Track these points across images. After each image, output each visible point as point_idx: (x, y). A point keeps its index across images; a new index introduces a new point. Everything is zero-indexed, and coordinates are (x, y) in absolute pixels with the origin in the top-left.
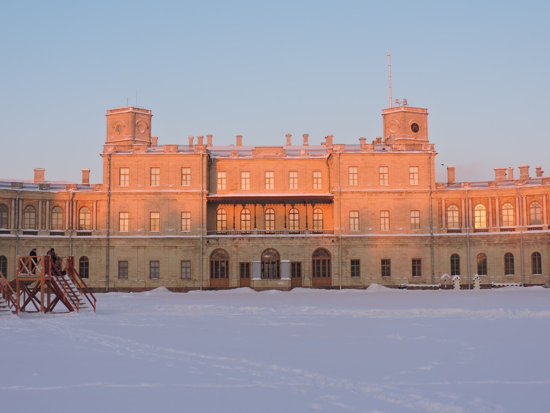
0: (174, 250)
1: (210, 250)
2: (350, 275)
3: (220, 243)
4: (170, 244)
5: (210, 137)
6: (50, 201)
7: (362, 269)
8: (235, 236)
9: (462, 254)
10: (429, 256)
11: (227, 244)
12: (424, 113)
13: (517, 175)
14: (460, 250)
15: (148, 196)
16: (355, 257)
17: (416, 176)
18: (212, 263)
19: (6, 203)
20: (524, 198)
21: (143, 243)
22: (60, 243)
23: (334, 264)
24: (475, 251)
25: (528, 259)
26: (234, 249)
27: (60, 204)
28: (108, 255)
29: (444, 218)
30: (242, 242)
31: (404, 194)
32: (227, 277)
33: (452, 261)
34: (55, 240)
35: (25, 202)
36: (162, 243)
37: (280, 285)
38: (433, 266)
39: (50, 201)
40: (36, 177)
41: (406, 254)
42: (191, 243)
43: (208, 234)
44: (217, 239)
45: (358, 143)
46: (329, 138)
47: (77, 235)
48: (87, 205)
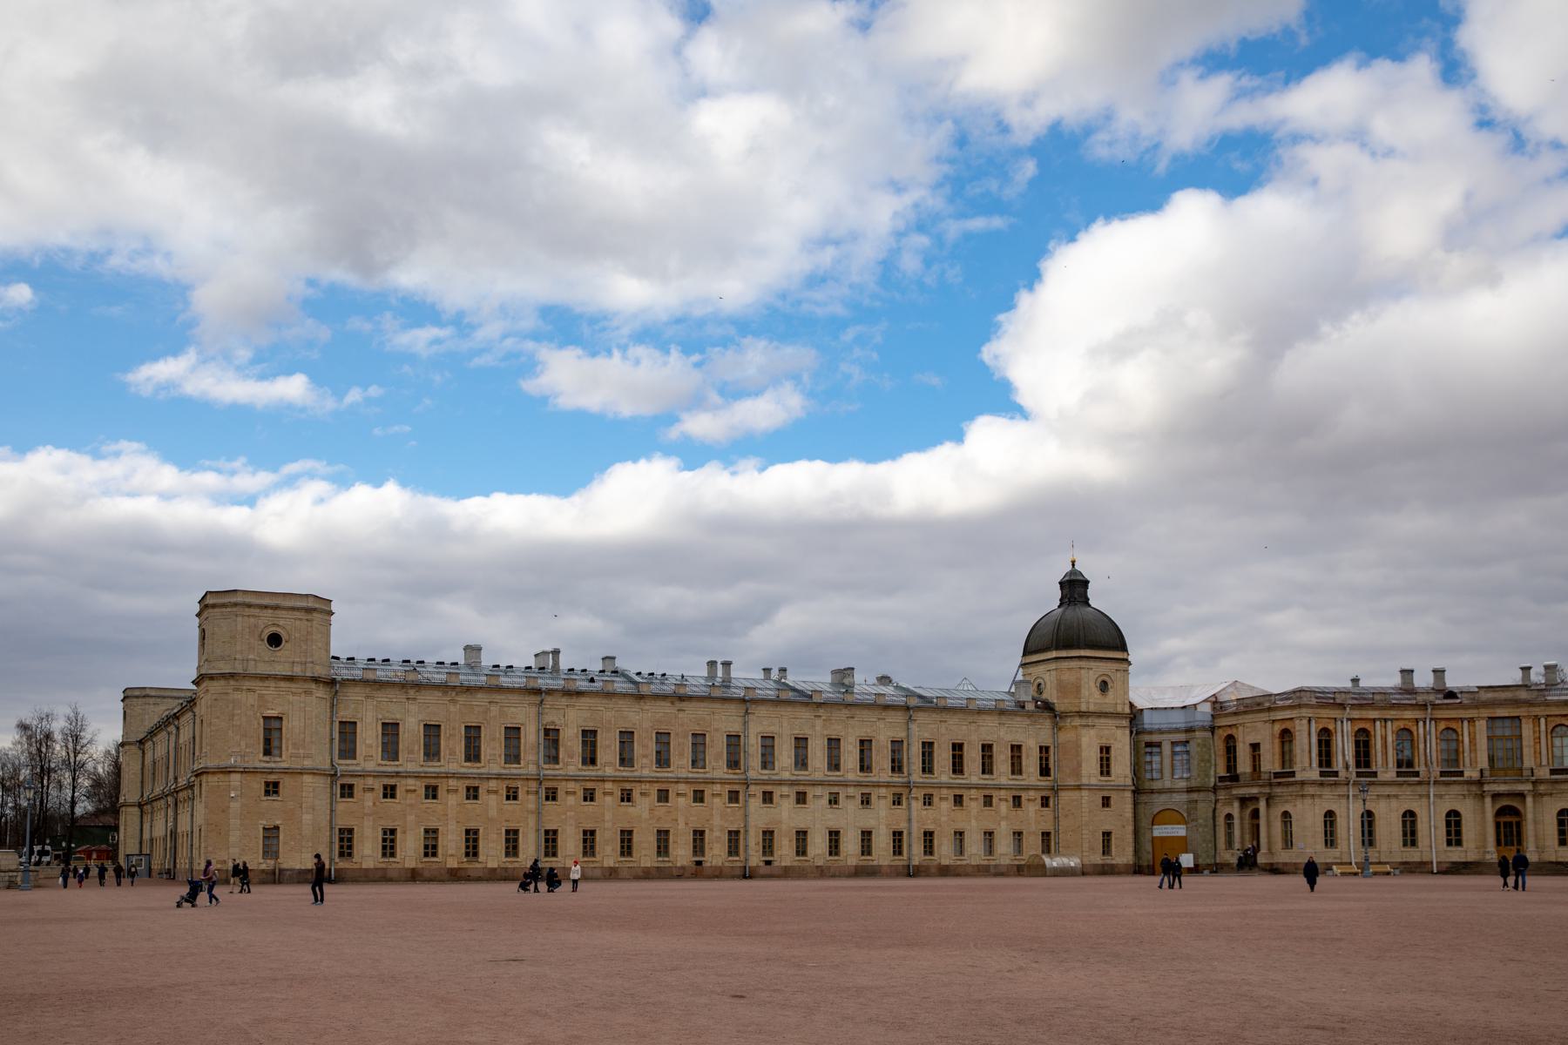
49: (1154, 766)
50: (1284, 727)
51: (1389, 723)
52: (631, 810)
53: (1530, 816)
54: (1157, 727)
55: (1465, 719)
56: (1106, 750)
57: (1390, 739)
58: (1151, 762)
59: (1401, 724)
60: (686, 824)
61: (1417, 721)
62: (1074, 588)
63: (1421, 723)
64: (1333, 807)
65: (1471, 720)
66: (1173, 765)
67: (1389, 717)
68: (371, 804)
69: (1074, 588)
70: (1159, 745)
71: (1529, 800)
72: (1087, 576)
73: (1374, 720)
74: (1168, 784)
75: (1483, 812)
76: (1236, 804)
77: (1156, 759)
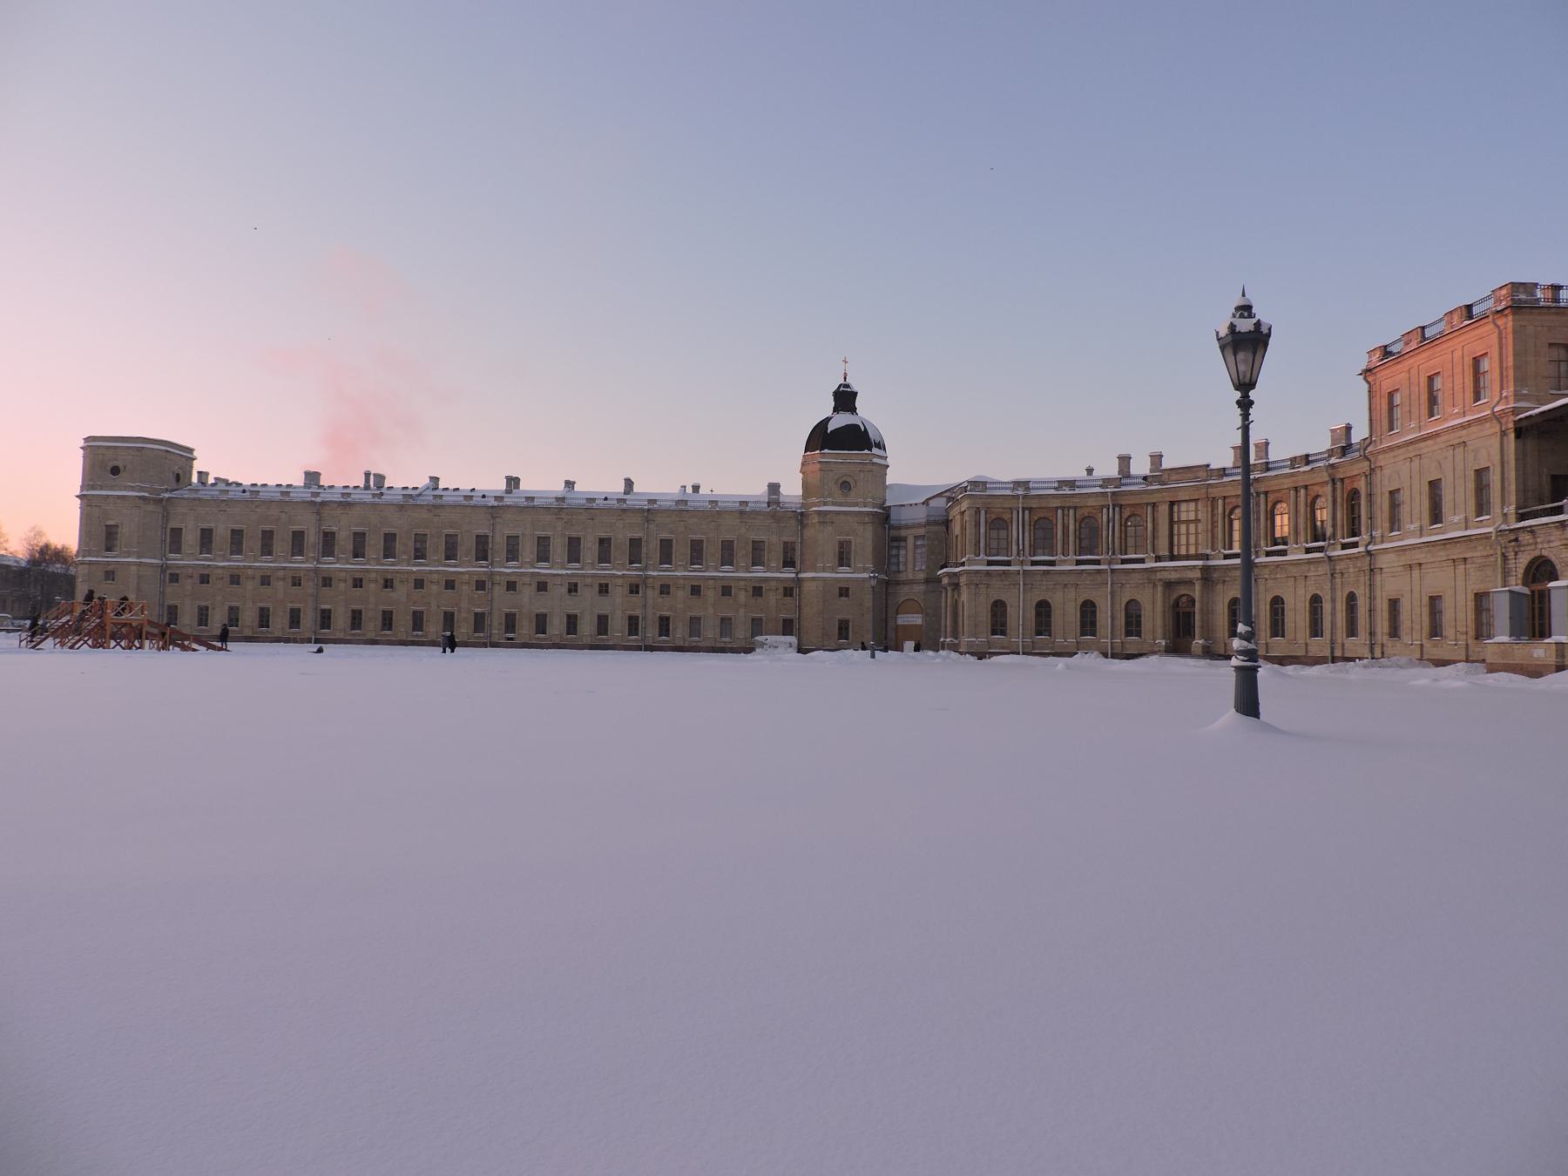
1: (1524, 560)
3: (1539, 540)
4: (1457, 552)
6: (1306, 487)
11: (1552, 541)
15: (1422, 445)
21: (1419, 556)
22: (1319, 569)
28: (1371, 586)
34: (1310, 562)
35: (1271, 498)
36: (1442, 553)
37: (1537, 659)
42: (1488, 548)
43: (1521, 517)
44: (1531, 530)
47: (1342, 549)
49: (901, 559)
52: (391, 594)
54: (903, 522)
55: (1150, 504)
57: (1071, 528)
58: (898, 555)
59: (1085, 512)
60: (438, 607)
61: (1103, 506)
62: (845, 399)
63: (1105, 510)
64: (1003, 598)
66: (914, 558)
67: (1071, 504)
68: (190, 588)
69: (845, 399)
70: (905, 539)
71: (1197, 587)
72: (855, 389)
73: (1057, 508)
74: (911, 577)
77: (902, 552)
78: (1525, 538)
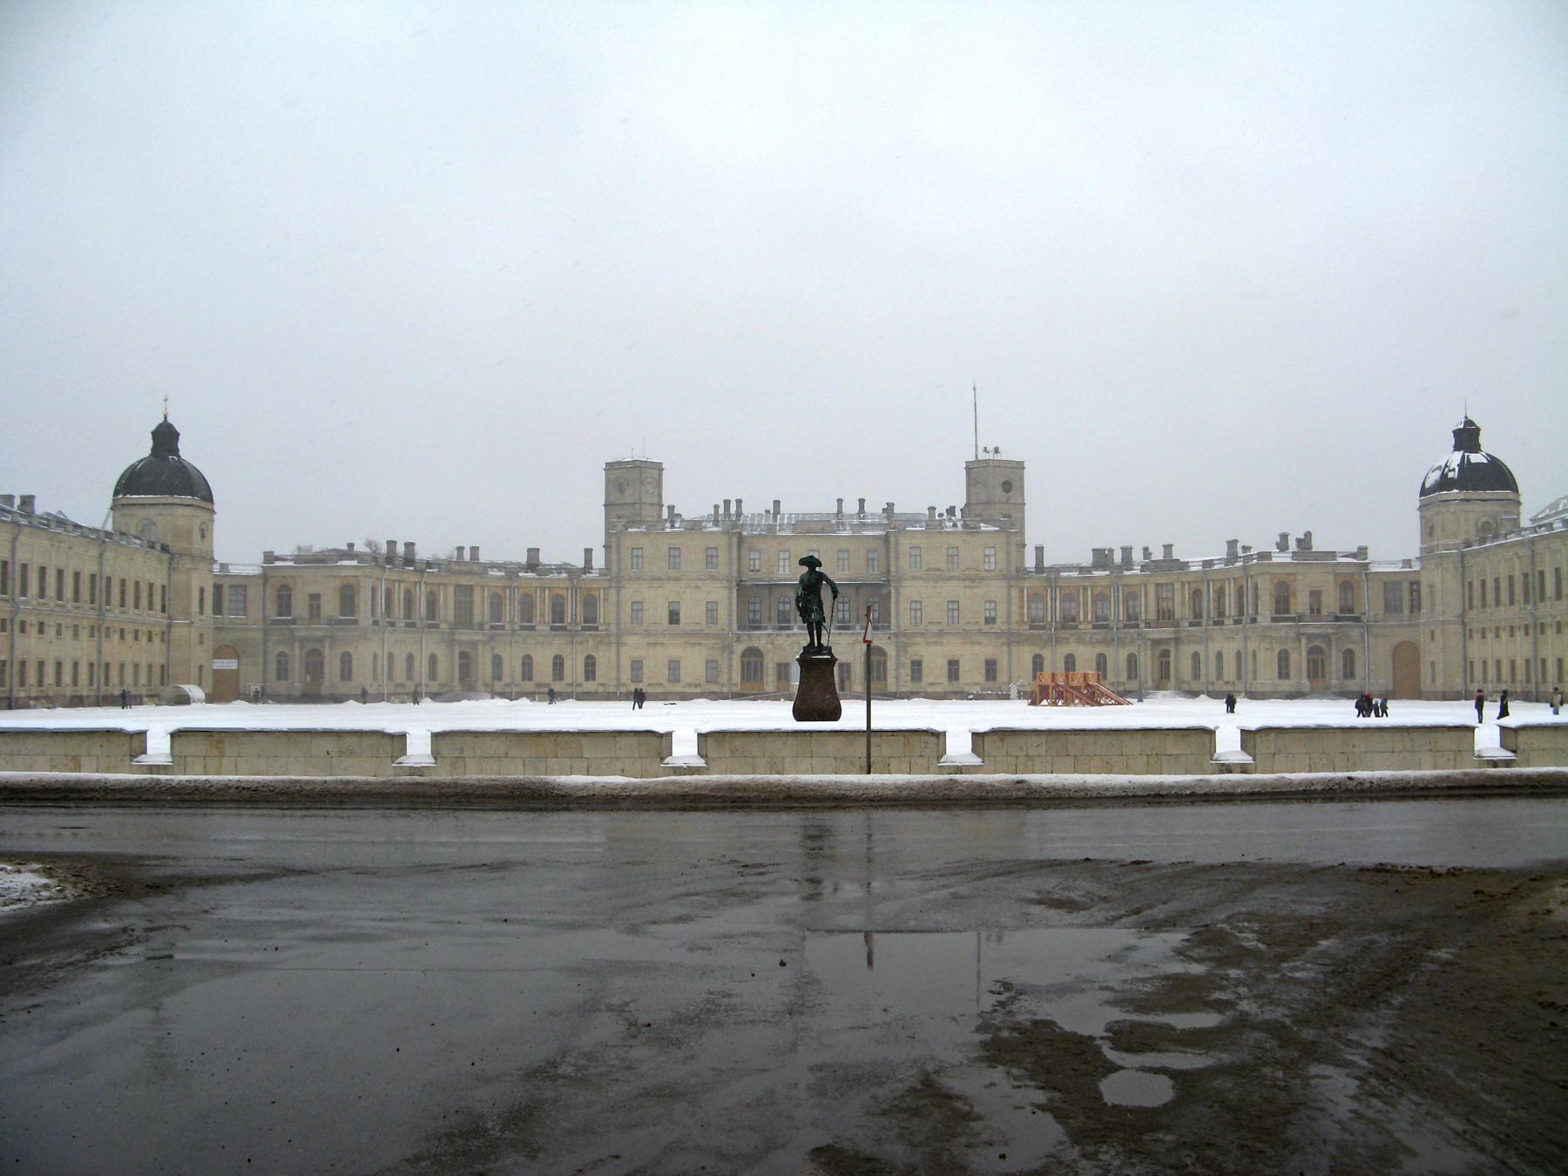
0: (697, 648)
2: (909, 678)
5: (739, 502)
6: (549, 588)
7: (925, 672)
8: (770, 631)
9: (1047, 654)
10: (1006, 656)
12: (1020, 466)
13: (1118, 558)
14: (1044, 650)
16: (915, 658)
17: (992, 559)
18: (743, 664)
19: (500, 592)
20: (1120, 588)
23: (891, 665)
24: (1063, 650)
25: (1123, 662)
26: (770, 647)
27: (561, 592)
28: (618, 654)
29: (1025, 610)
30: (779, 638)
31: (977, 581)
32: (762, 679)
33: (1035, 662)
35: (521, 590)
38: (1010, 668)
39: (549, 588)
40: (529, 557)
41: (978, 654)
45: (927, 512)
46: (890, 506)
48: (592, 593)
50: (345, 582)
51: (402, 585)
53: (480, 659)
56: (202, 591)
61: (416, 583)
62: (165, 437)
63: (418, 585)
65: (445, 585)
69: (165, 437)
71: (480, 647)
72: (178, 429)
73: (395, 581)
75: (452, 652)
76: (297, 645)
78: (742, 638)
